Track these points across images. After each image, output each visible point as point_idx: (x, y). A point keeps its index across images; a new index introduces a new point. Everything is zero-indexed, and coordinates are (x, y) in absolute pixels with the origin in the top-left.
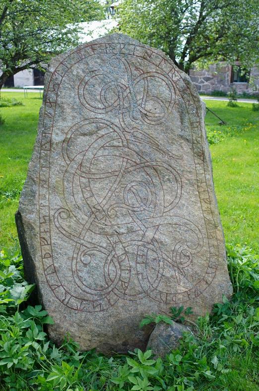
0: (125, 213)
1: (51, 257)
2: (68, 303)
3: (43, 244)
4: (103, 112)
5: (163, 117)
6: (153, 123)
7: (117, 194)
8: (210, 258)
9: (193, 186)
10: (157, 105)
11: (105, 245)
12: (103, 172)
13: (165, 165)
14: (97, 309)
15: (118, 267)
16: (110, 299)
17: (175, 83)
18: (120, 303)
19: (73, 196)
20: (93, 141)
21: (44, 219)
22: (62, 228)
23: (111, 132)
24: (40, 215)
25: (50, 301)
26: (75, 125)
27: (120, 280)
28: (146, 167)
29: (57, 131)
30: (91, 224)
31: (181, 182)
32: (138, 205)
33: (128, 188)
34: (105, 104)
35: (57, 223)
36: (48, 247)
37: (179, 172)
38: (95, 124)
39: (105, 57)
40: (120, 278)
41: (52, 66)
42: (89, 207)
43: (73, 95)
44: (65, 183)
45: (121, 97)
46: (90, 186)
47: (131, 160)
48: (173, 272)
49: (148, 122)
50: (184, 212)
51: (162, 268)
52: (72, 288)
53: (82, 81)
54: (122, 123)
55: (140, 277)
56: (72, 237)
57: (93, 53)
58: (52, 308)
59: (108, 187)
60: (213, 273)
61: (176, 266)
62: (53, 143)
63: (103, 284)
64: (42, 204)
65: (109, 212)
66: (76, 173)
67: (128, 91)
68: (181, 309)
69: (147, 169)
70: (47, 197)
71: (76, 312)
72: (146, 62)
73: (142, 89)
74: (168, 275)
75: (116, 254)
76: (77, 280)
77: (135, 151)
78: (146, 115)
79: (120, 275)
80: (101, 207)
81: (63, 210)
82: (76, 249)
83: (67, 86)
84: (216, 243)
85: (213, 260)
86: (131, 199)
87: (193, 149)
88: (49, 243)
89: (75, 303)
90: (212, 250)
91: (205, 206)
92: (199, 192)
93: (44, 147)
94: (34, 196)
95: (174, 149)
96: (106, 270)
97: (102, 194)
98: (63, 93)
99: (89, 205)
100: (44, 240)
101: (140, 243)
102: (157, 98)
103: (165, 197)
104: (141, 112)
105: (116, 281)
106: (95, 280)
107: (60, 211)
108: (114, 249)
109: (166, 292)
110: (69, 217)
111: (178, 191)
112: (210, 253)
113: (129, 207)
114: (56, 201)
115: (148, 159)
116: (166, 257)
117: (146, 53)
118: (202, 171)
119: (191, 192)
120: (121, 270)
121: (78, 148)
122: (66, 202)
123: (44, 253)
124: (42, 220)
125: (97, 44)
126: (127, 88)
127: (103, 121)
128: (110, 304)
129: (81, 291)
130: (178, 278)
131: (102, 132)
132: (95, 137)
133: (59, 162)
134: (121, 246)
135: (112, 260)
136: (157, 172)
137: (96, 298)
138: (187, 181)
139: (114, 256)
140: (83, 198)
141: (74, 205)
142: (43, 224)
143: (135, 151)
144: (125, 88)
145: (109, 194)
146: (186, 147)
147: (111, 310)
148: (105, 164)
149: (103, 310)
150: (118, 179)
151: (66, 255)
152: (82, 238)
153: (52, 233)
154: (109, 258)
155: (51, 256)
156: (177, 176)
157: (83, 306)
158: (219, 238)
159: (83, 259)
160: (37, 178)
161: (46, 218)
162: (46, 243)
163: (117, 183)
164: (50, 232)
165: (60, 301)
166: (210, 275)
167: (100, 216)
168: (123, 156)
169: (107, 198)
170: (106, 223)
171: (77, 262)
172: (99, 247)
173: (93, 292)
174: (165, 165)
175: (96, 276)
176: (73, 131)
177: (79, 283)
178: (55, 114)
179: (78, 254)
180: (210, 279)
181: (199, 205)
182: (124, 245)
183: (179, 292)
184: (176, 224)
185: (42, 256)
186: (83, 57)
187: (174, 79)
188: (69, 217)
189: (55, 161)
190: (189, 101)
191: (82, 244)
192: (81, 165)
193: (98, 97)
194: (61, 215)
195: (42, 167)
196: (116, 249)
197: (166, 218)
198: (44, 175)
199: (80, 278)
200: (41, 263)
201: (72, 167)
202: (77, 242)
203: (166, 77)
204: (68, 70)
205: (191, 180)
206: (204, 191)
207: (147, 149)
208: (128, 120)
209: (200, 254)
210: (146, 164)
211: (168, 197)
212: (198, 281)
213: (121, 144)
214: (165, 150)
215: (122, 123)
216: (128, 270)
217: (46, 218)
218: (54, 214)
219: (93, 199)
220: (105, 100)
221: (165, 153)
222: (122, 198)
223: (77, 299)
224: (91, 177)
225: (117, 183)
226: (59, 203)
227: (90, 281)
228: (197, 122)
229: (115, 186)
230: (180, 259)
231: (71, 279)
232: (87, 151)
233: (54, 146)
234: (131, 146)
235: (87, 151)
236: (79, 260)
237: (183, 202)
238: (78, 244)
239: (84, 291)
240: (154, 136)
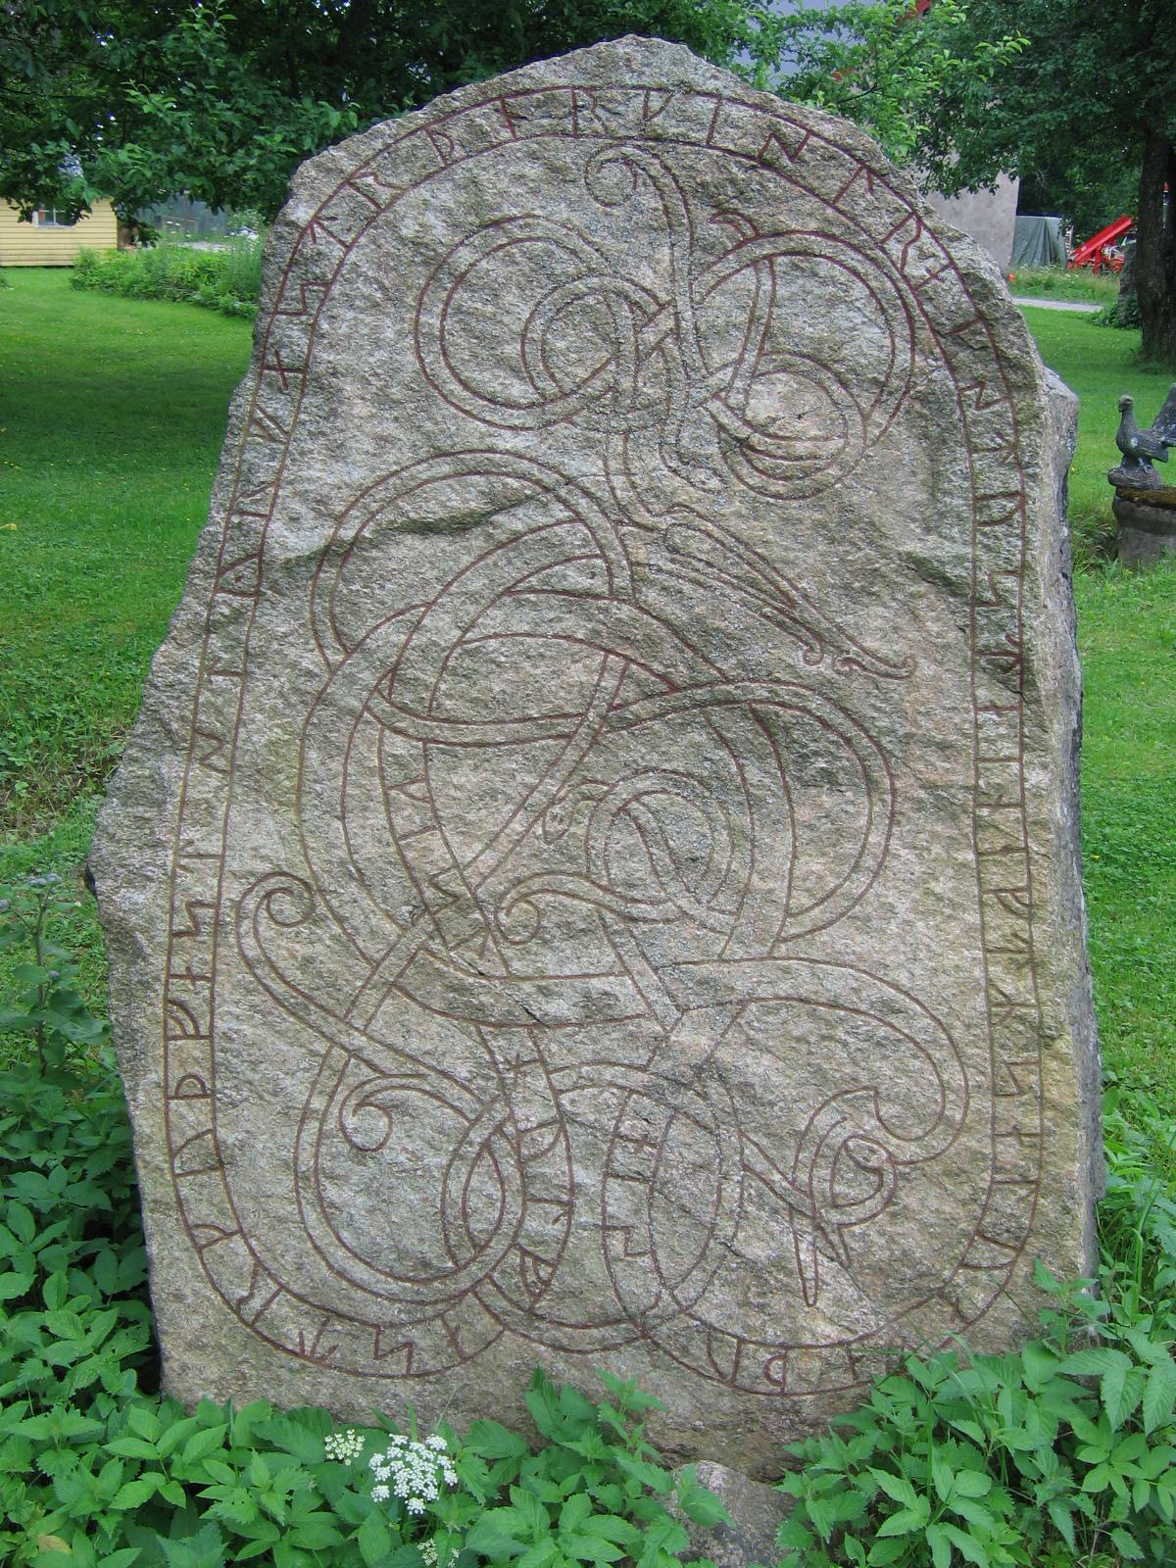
1: (205, 1096)
2: (259, 1315)
3: (179, 1032)
5: (834, 458)
6: (779, 487)
7: (554, 827)
8: (990, 1193)
9: (954, 817)
10: (810, 399)
11: (462, 1071)
12: (500, 713)
13: (815, 703)
15: (516, 1182)
16: (457, 1328)
19: (342, 818)
20: (466, 560)
21: (193, 917)
22: (274, 968)
23: (559, 523)
25: (179, 1297)
26: (383, 480)
27: (514, 1245)
28: (719, 703)
29: (298, 507)
30: (412, 959)
31: (894, 791)
33: (613, 804)
35: (249, 942)
36: (195, 1049)
37: (884, 741)
40: (516, 1235)
41: (303, 193)
43: (390, 334)
44: (313, 755)
45: (628, 349)
46: (426, 779)
49: (755, 480)
52: (287, 1249)
54: (618, 481)
57: (506, 134)
60: (1002, 1267)
63: (432, 1251)
64: (190, 843)
65: (502, 916)
66: (367, 708)
67: (666, 322)
69: (717, 714)
70: (221, 812)
71: (296, 1363)
72: (775, 185)
73: (742, 318)
74: (758, 1251)
75: (511, 1117)
76: (312, 1216)
77: (667, 623)
78: (744, 444)
80: (467, 885)
81: (284, 881)
82: (326, 1073)
83: (366, 290)
84: (1032, 1122)
85: (1008, 1203)
86: (628, 860)
87: (971, 629)
88: (204, 1031)
89: (296, 1328)
92: (979, 854)
93: (231, 575)
94: (160, 804)
95: (875, 628)
96: (455, 1187)
97: (481, 821)
98: (343, 321)
99: (408, 868)
100: (181, 1015)
101: (639, 1079)
102: (820, 363)
104: (721, 427)
105: (498, 1246)
107: (273, 883)
110: (309, 916)
112: (996, 1170)
114: (261, 837)
115: (728, 665)
116: (760, 1165)
117: (776, 134)
118: (1009, 748)
119: (936, 849)
120: (528, 1198)
122: (305, 847)
123: (176, 1073)
126: (662, 307)
127: (525, 465)
128: (460, 1352)
129: (325, 1272)
132: (476, 541)
134: (541, 1084)
135: (486, 1146)
136: (770, 735)
137: (394, 1312)
138: (922, 794)
139: (499, 1129)
140: (387, 836)
141: (342, 863)
142: (187, 941)
143: (667, 623)
144: (654, 308)
147: (459, 1378)
149: (422, 1375)
150: (571, 755)
151: (275, 1094)
152: (359, 1023)
153: (224, 988)
154: (477, 1136)
158: (1053, 1094)
159: (351, 1122)
160: (183, 718)
161: (199, 911)
162: (191, 1030)
164: (212, 980)
165: (227, 1302)
166: (983, 1276)
168: (605, 642)
169: (504, 844)
171: (321, 1134)
174: (815, 703)
175: (404, 1211)
176: (374, 506)
177: (319, 1230)
178: (298, 423)
181: (973, 918)
182: (554, 1076)
183: (807, 1339)
184: (833, 1005)
185: (166, 1086)
186: (458, 152)
188: (309, 916)
189: (275, 646)
191: (355, 1053)
192: (394, 670)
194: (274, 907)
196: (517, 1095)
197: (786, 971)
198: (219, 711)
200: (159, 1119)
201: (351, 680)
203: (873, 260)
205: (948, 787)
206: (1007, 849)
207: (734, 613)
208: (652, 462)
209: (937, 1169)
211: (813, 864)
212: (914, 1300)
213: (599, 585)
215: (618, 481)
216: (560, 1202)
219: (434, 841)
220: (544, 359)
223: (306, 1307)
224: (439, 733)
227: (373, 1231)
228: (1009, 495)
229: (551, 786)
232: (429, 605)
234: (651, 596)
235: (429, 605)
236: (331, 1124)
238: (337, 1051)
239: (341, 1274)
240: (776, 553)
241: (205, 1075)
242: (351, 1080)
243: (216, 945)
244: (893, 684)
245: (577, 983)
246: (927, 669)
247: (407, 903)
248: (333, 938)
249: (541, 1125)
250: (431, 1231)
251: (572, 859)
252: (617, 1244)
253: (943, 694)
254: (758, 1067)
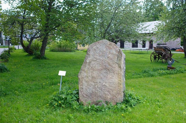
10: (112, 55)
11: (93, 85)
18: (94, 98)
36: (82, 83)
39: (101, 44)
50: (113, 80)
52: (85, 92)
55: (100, 93)
61: (108, 91)
63: (91, 93)
68: (108, 102)
72: (110, 45)
74: (106, 93)
76: (86, 91)
84: (120, 88)
86: (102, 76)
89: (85, 96)
90: (118, 89)
91: (119, 79)
95: (114, 66)
97: (95, 74)
98: (90, 52)
101: (101, 85)
103: (109, 76)
105: (94, 92)
108: (95, 86)
110: (87, 78)
114: (85, 74)
118: (120, 71)
121: (92, 64)
135: (94, 88)
137: (89, 95)
146: (117, 65)
147: (92, 99)
156: (114, 72)
173: (89, 94)
177: (87, 92)
180: (117, 96)
181: (118, 79)
188: (87, 78)
193: (98, 53)
199: (87, 91)
204: (92, 47)
208: (104, 58)
211: (110, 76)
226: (86, 75)
227: (89, 92)
237: (114, 78)
240: (109, 62)
246: (116, 67)
250: (91, 92)
252: (100, 93)
253: (117, 68)
254: (107, 85)
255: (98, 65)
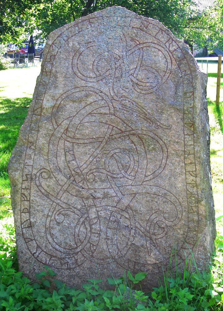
0: (103, 179)
1: (28, 212)
2: (38, 256)
3: (23, 199)
4: (94, 80)
6: (144, 92)
8: (187, 232)
10: (150, 75)
11: (79, 207)
12: (87, 137)
14: (64, 267)
15: (89, 229)
17: (171, 53)
24: (24, 173)
25: (22, 253)
26: (66, 92)
27: (89, 242)
29: (48, 97)
32: (118, 172)
34: (97, 73)
35: (37, 182)
36: (27, 203)
37: (165, 141)
38: (84, 92)
42: (70, 169)
44: (51, 146)
46: (73, 150)
47: (116, 127)
48: (145, 242)
49: (139, 91)
51: (133, 236)
53: (77, 52)
56: (50, 197)
58: (24, 259)
59: (91, 152)
62: (44, 108)
64: (27, 163)
66: (62, 136)
69: (131, 137)
70: (33, 157)
74: (138, 244)
75: (88, 217)
76: (49, 237)
77: (121, 119)
78: (137, 84)
79: (90, 237)
81: (45, 170)
86: (113, 166)
87: (183, 119)
88: (28, 199)
92: (185, 164)
96: (77, 230)
97: (84, 157)
100: (24, 196)
101: (114, 209)
106: (65, 239)
109: (135, 261)
110: (50, 177)
111: (163, 161)
112: (189, 228)
113: (109, 173)
114: (41, 162)
115: (134, 127)
116: (139, 226)
119: (176, 163)
121: (66, 114)
123: (23, 208)
124: (25, 178)
125: (94, 18)
127: (92, 89)
129: (51, 248)
130: (149, 249)
131: (90, 100)
133: (47, 126)
135: (84, 222)
136: (142, 141)
139: (86, 218)
142: (26, 182)
143: (121, 119)
145: (91, 159)
148: (90, 130)
149: (70, 269)
150: (102, 145)
153: (32, 191)
154: (82, 220)
155: (29, 212)
156: (163, 146)
157: (51, 261)
159: (57, 217)
160: (26, 139)
161: (28, 176)
162: (26, 199)
163: (100, 148)
164: (30, 189)
165: (31, 253)
167: (78, 179)
168: (109, 123)
169: (88, 163)
170: (83, 187)
171: (51, 220)
172: (73, 209)
176: (64, 98)
177: (50, 239)
179: (53, 212)
182: (97, 209)
185: (21, 210)
187: (170, 49)
190: (185, 71)
191: (58, 204)
194: (43, 175)
195: (32, 130)
197: (145, 187)
199: (52, 235)
200: (19, 217)
202: (53, 202)
203: (163, 47)
205: (178, 150)
206: (191, 163)
210: (131, 132)
213: (108, 112)
214: (153, 119)
215: (111, 92)
216: (97, 233)
217: (28, 176)
218: (37, 173)
221: (152, 122)
222: (102, 163)
225: (100, 148)
226: (43, 164)
227: (61, 238)
229: (98, 151)
230: (154, 230)
231: (43, 234)
232: (74, 116)
233: (44, 111)
235: (74, 116)
236: (53, 218)
238: (54, 204)
241: (28, 208)
242: (57, 209)
243: (31, 182)
244: (166, 130)
245: (103, 190)
247: (69, 174)
248: (54, 181)
249: (94, 218)
250: (71, 238)
251: (102, 166)
252: (109, 242)
255: (93, 119)
